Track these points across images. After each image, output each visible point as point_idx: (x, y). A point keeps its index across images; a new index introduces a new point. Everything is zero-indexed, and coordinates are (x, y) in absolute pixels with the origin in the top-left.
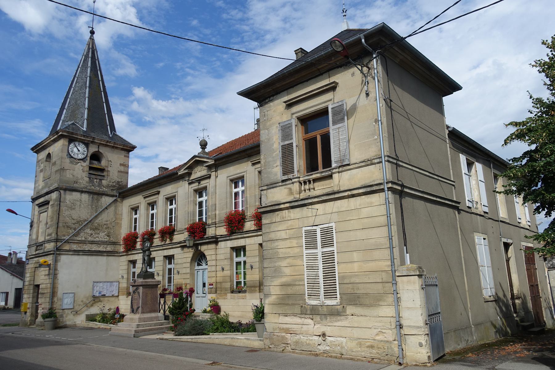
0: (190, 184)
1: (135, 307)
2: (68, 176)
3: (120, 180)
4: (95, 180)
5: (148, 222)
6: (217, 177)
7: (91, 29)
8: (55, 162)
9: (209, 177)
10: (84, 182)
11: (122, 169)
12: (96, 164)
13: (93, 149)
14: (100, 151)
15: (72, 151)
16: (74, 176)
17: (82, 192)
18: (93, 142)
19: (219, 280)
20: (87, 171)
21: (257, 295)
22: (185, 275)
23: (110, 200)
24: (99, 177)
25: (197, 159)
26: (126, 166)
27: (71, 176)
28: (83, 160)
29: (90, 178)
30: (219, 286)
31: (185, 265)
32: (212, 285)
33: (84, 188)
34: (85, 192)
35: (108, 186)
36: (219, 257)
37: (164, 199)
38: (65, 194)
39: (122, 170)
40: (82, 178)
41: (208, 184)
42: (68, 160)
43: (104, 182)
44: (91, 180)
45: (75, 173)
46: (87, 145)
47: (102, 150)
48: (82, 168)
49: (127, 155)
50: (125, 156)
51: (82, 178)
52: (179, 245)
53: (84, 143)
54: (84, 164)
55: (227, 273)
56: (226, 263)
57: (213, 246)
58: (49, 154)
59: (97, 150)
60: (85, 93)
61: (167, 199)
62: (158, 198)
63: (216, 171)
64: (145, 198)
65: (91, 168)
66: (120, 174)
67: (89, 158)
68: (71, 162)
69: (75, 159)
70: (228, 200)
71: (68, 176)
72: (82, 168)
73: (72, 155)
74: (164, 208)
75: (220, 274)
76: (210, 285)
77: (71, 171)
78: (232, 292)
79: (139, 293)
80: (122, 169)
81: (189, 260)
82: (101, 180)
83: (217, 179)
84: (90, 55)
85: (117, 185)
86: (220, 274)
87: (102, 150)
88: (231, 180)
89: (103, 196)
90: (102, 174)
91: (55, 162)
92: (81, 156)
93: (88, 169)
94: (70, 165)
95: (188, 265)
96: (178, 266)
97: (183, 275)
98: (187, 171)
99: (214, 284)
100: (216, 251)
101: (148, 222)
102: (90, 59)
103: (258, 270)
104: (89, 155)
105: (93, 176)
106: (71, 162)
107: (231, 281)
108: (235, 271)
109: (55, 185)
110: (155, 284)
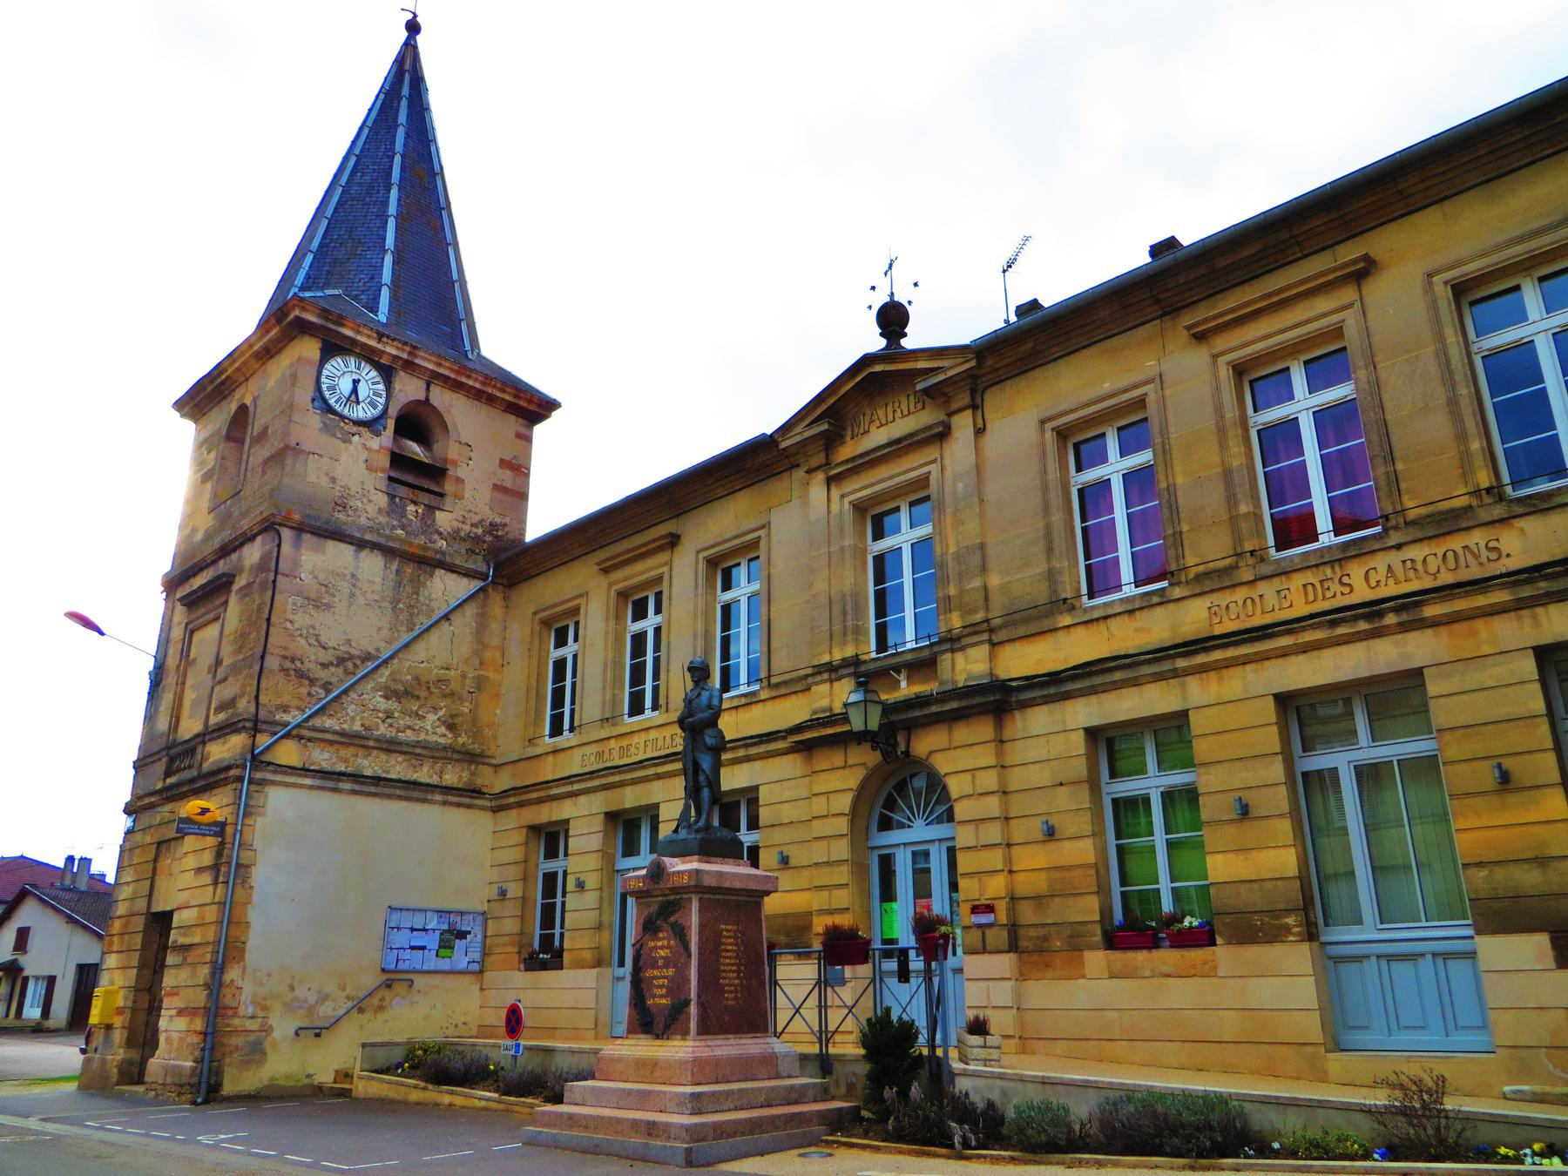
0: (830, 481)
1: (659, 1000)
2: (312, 478)
3: (498, 520)
4: (411, 508)
5: (617, 665)
6: (980, 431)
7: (410, 16)
8: (266, 428)
9: (941, 435)
10: (372, 511)
11: (507, 478)
12: (414, 449)
13: (409, 389)
14: (434, 401)
15: (332, 388)
16: (333, 480)
17: (361, 544)
18: (409, 366)
19: (1027, 884)
20: (383, 471)
21: (1296, 956)
22: (825, 870)
23: (461, 587)
24: (425, 498)
25: (878, 368)
26: (519, 468)
27: (324, 482)
28: (371, 425)
29: (392, 497)
30: (1027, 914)
31: (819, 828)
32: (990, 909)
33: (371, 529)
34: (374, 546)
35: (454, 536)
36: (1017, 779)
37: (702, 566)
38: (297, 543)
39: (508, 484)
40: (364, 494)
41: (934, 469)
42: (314, 419)
43: (444, 520)
44: (395, 508)
45: (339, 471)
46: (387, 374)
47: (441, 398)
48: (365, 455)
49: (524, 431)
50: (518, 436)
51: (364, 494)
52: (781, 745)
53: (378, 366)
54: (375, 443)
55: (1081, 851)
56: (1071, 808)
57: (982, 730)
58: (243, 409)
59: (422, 396)
60: (385, 204)
61: (712, 563)
62: (670, 563)
63: (975, 407)
64: (606, 571)
65: (399, 460)
66: (500, 496)
67: (391, 424)
68: (327, 428)
69: (343, 417)
70: (1057, 518)
71: (312, 478)
72: (365, 455)
73: (332, 402)
74: (701, 601)
75: (1032, 859)
76: (975, 910)
77: (326, 460)
78: (1113, 940)
79: (681, 933)
80: (507, 478)
81: (844, 803)
82: (431, 509)
83: (988, 440)
84: (405, 91)
85: (488, 538)
86: (1032, 859)
87: (441, 398)
88: (1062, 434)
89: (439, 572)
90: (434, 488)
91: (266, 428)
92: (363, 412)
93: (387, 464)
94: (324, 438)
95: (842, 825)
96: (778, 836)
97: (806, 873)
98: (825, 427)
99: (1002, 907)
100: (999, 754)
101: (617, 665)
102: (404, 103)
103: (1285, 827)
104: (393, 411)
105: (402, 491)
106: (327, 428)
107: (1103, 890)
108: (1112, 842)
109: (260, 511)
110: (752, 886)
